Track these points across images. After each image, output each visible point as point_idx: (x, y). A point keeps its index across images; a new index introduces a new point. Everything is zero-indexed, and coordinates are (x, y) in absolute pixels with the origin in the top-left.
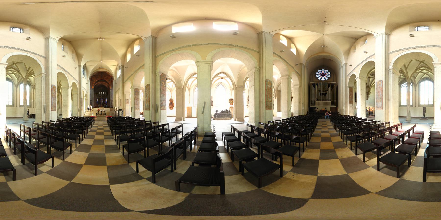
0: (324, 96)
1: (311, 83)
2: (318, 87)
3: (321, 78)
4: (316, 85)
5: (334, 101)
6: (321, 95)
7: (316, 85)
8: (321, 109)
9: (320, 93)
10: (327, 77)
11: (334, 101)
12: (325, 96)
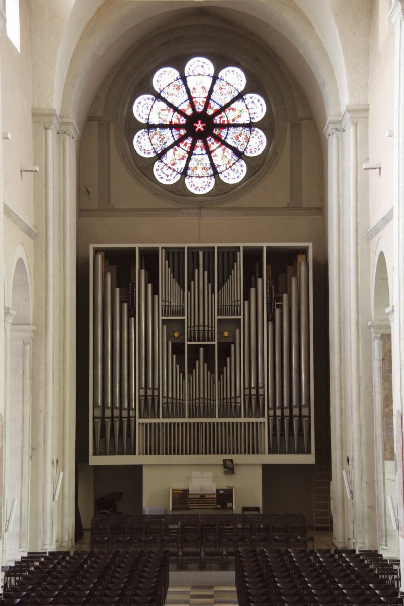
0: (211, 369)
1: (97, 251)
2: (155, 291)
3: (181, 165)
4: (140, 275)
5: (296, 411)
6: (180, 362)
7: (140, 275)
8: (180, 486)
9: (178, 349)
10: (235, 151)
11: (291, 416)
12: (221, 372)
